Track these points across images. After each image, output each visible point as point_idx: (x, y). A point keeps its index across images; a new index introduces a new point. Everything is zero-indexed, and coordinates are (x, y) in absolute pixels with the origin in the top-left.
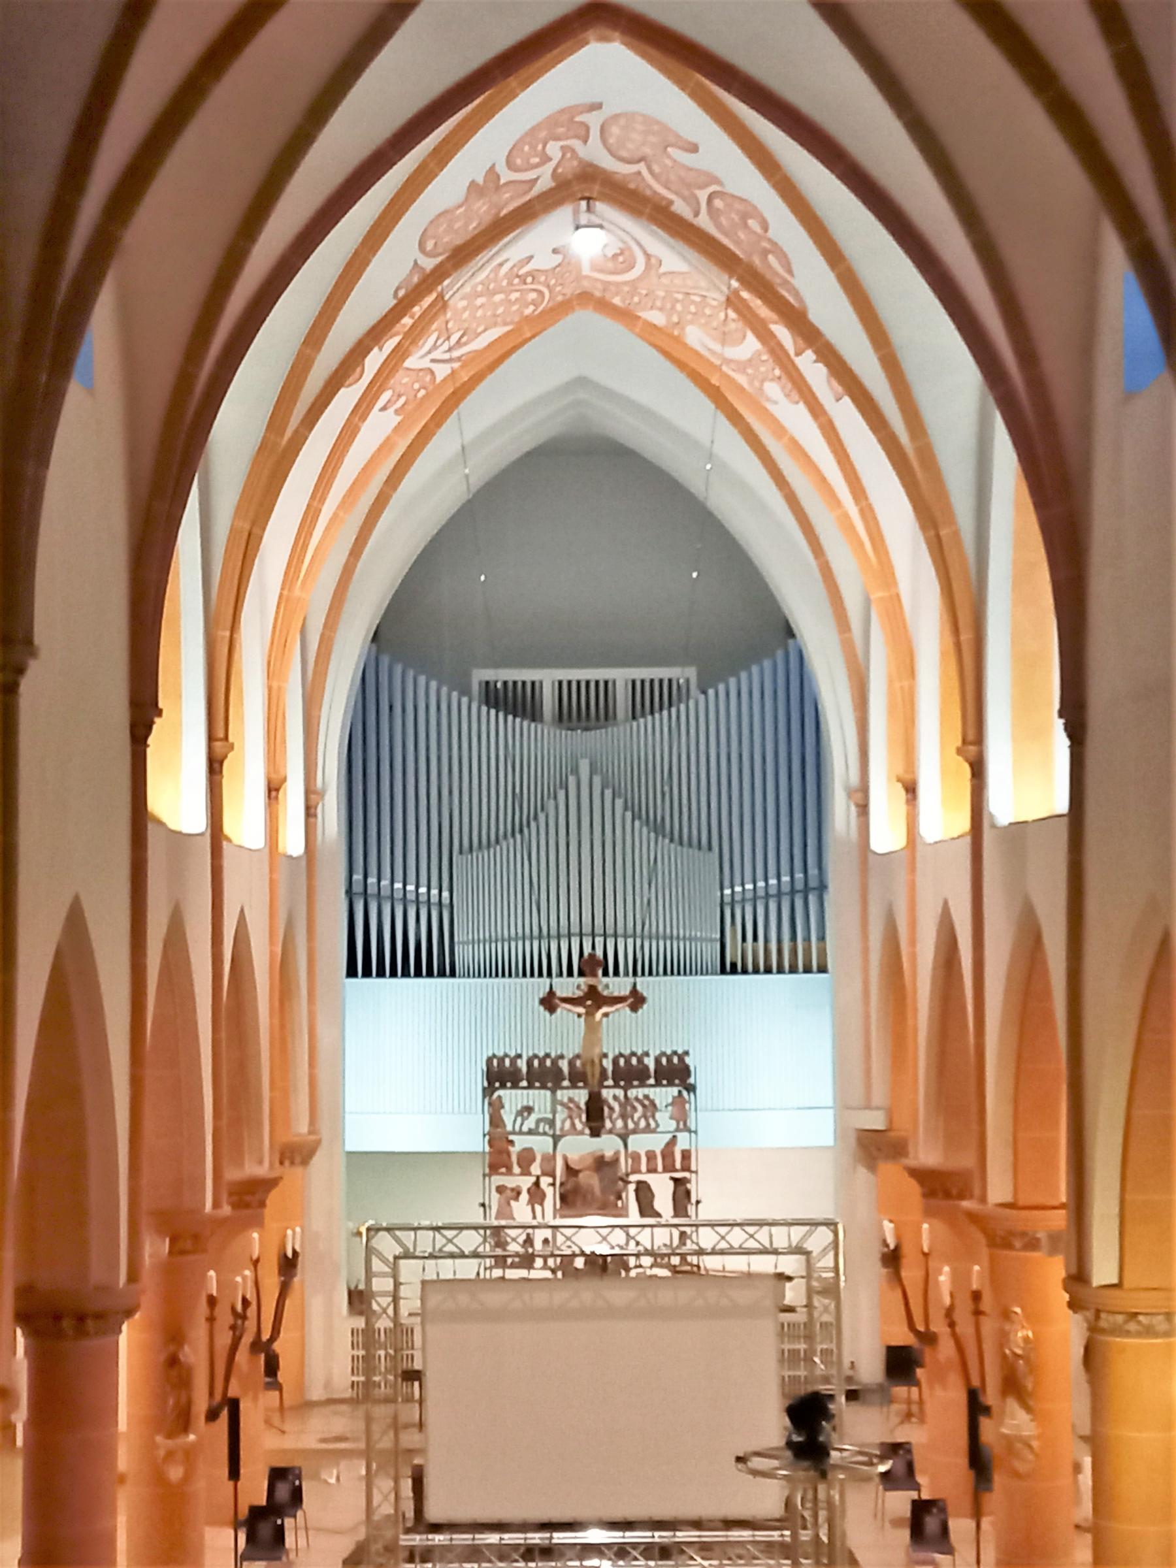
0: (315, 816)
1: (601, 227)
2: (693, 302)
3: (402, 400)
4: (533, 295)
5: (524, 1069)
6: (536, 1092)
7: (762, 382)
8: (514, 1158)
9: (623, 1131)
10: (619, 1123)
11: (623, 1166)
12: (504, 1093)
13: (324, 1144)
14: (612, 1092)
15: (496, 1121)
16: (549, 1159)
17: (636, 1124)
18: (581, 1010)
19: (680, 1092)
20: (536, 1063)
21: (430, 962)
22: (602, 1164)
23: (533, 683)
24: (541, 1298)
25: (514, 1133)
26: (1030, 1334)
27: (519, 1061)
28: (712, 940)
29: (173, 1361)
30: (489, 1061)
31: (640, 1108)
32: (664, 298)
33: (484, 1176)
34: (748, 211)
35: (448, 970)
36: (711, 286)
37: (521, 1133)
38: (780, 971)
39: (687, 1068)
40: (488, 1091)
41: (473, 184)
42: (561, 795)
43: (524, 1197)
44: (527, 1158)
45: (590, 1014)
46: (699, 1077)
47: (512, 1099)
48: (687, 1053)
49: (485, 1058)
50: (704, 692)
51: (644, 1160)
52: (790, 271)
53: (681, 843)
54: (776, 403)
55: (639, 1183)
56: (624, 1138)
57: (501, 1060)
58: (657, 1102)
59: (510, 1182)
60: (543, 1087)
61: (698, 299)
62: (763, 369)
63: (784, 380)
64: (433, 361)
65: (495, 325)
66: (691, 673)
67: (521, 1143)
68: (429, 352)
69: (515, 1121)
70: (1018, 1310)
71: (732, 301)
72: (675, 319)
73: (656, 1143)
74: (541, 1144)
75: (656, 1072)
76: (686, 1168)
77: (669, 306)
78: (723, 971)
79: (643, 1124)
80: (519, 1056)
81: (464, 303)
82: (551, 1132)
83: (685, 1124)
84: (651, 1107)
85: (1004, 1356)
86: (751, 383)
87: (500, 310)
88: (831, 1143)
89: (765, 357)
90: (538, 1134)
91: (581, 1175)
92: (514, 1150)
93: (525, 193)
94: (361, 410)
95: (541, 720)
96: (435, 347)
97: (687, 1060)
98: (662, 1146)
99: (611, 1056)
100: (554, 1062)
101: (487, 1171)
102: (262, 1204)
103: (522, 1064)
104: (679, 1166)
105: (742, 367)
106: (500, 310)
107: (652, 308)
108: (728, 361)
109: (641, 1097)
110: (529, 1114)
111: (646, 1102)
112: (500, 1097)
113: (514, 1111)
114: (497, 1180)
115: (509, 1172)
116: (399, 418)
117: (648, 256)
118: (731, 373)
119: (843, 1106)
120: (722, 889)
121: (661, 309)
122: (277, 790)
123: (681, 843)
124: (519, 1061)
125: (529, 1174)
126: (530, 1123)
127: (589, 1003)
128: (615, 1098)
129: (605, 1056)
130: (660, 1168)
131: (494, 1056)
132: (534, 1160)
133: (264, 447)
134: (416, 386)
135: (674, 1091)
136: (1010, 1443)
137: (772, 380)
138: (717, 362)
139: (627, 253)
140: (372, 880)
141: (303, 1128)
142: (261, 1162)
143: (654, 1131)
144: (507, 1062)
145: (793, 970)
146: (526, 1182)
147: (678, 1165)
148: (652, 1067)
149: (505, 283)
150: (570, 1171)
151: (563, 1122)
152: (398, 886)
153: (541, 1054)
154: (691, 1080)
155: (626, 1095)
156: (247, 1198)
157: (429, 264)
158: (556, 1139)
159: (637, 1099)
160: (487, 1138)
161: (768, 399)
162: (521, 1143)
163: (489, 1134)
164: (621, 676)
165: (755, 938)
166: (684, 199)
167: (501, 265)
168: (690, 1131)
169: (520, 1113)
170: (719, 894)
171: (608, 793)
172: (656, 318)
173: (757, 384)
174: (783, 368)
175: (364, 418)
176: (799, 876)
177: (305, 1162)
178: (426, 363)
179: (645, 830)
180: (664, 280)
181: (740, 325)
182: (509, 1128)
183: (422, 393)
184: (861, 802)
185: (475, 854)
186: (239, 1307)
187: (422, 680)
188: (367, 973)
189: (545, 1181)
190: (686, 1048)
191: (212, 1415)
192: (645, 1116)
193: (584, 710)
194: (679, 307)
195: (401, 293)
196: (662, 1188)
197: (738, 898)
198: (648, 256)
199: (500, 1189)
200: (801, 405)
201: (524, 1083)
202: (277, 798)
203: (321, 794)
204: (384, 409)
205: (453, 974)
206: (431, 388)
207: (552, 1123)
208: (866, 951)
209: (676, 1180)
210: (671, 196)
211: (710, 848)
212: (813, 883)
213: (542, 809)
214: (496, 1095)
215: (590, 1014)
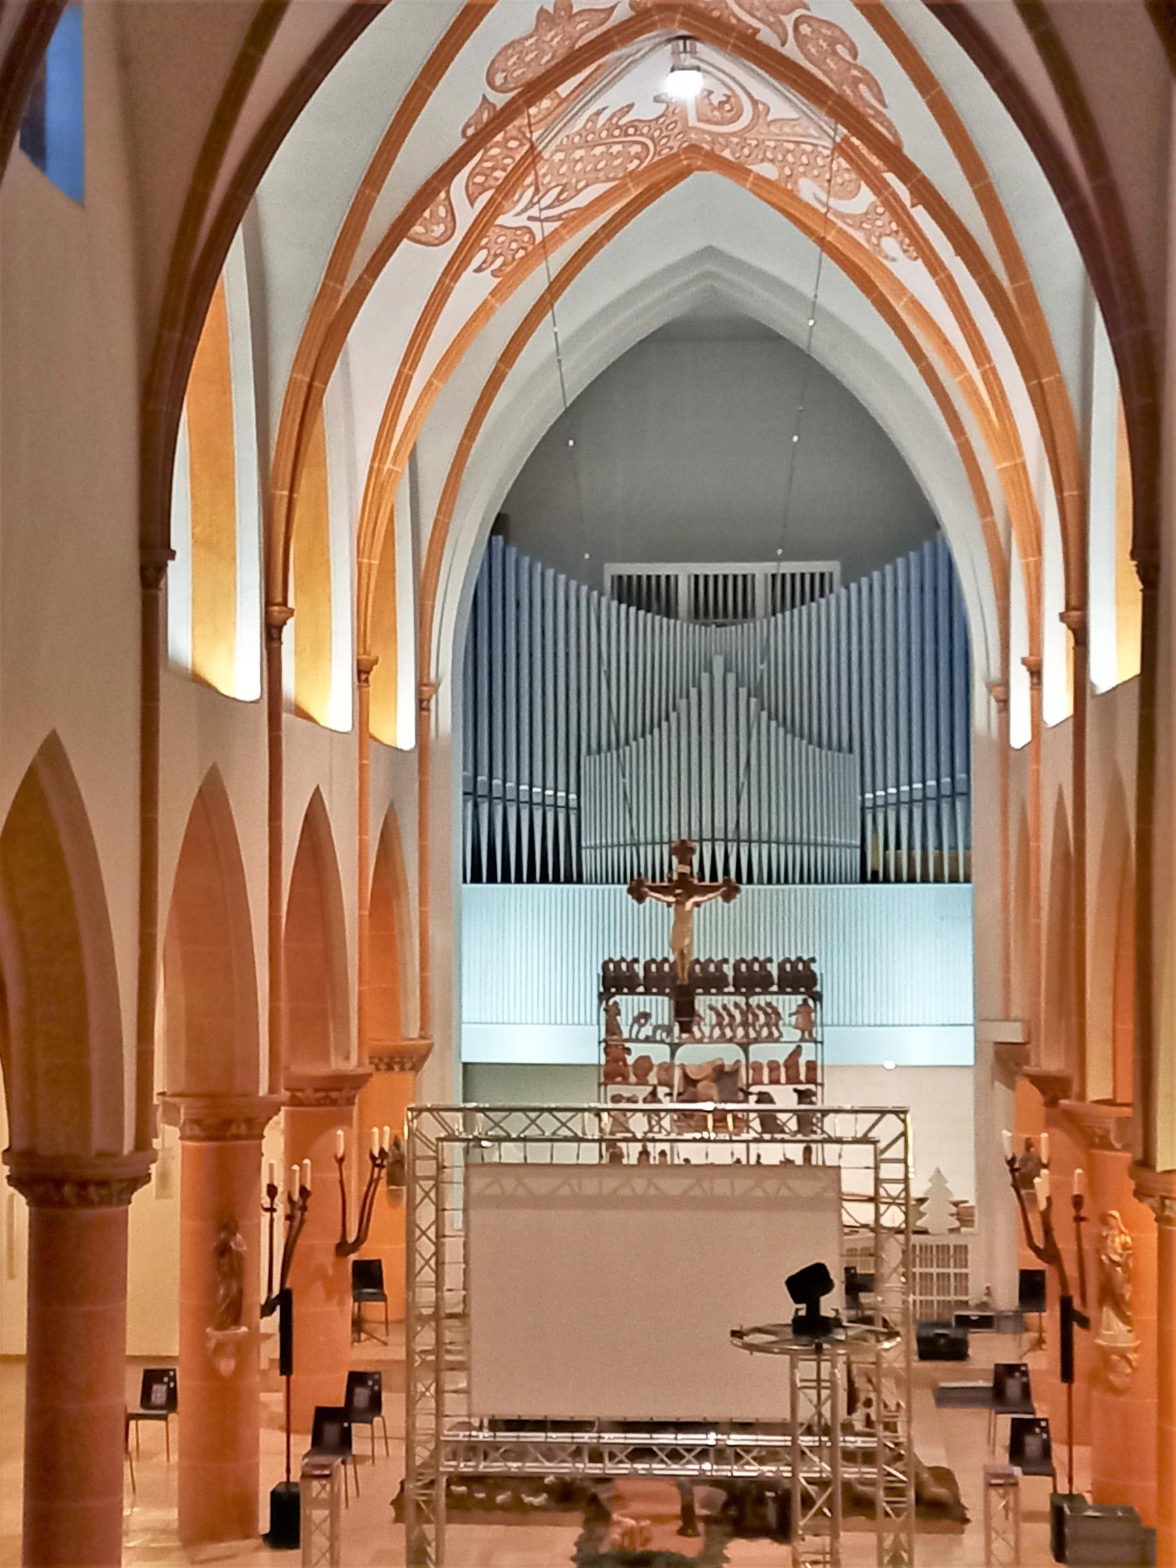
0: (428, 709)
1: (698, 69)
2: (804, 152)
3: (500, 260)
4: (636, 149)
5: (641, 974)
6: (654, 998)
7: (879, 238)
9: (745, 1040)
10: (740, 1032)
14: (733, 998)
15: (612, 1028)
17: (758, 1033)
18: (671, 899)
19: (805, 1001)
20: (653, 968)
21: (556, 867)
23: (668, 577)
24: (590, 1186)
25: (630, 1040)
26: (1129, 1240)
27: (636, 966)
28: (850, 846)
29: (224, 1250)
30: (605, 965)
31: (762, 1018)
32: (775, 148)
33: (600, 1085)
34: (837, 37)
36: (820, 133)
37: (637, 1040)
38: (925, 880)
39: (813, 975)
40: (604, 996)
41: (542, 11)
42: (693, 692)
44: (644, 1065)
45: (680, 903)
46: (825, 986)
47: (628, 1005)
48: (813, 960)
49: (601, 962)
50: (847, 588)
51: (766, 1071)
52: (882, 102)
53: (820, 745)
54: (894, 260)
55: (760, 1094)
56: (745, 1047)
57: (617, 964)
58: (780, 1010)
60: (661, 993)
61: (809, 148)
62: (879, 223)
63: (901, 234)
64: (530, 218)
65: (597, 180)
66: (832, 567)
67: (637, 1051)
68: (526, 209)
69: (632, 1026)
70: (1116, 1213)
71: (840, 149)
72: (787, 171)
73: (781, 1053)
74: (659, 1054)
75: (779, 978)
76: (811, 1080)
77: (780, 157)
78: (863, 880)
79: (765, 1032)
80: (636, 960)
81: (560, 156)
82: (668, 1040)
83: (810, 1034)
84: (773, 1015)
85: (1101, 1262)
86: (868, 241)
87: (601, 165)
88: (970, 1060)
89: (880, 210)
90: (656, 1042)
91: (700, 1085)
92: (630, 1060)
93: (601, 24)
94: (453, 271)
95: (676, 618)
96: (531, 204)
97: (814, 967)
98: (786, 1056)
99: (732, 961)
101: (602, 1079)
102: (350, 1102)
103: (639, 969)
104: (805, 1078)
105: (858, 222)
106: (601, 165)
107: (762, 161)
108: (843, 216)
109: (763, 1004)
111: (769, 1011)
112: (616, 1003)
113: (630, 1021)
114: (613, 1090)
115: (625, 1080)
116: (498, 280)
117: (755, 102)
118: (851, 231)
119: (981, 1018)
120: (863, 793)
121: (772, 161)
122: (368, 673)
123: (820, 745)
124: (636, 966)
125: (646, 1084)
126: (647, 1031)
127: (678, 891)
128: (736, 1005)
129: (726, 961)
130: (783, 1079)
131: (611, 960)
133: (325, 295)
134: (514, 246)
135: (800, 999)
136: (1105, 1355)
137: (889, 235)
138: (823, 210)
139: (732, 99)
140: (497, 782)
141: (414, 1032)
142: (347, 1058)
143: (777, 1041)
144: (624, 966)
145: (939, 879)
147: (802, 1077)
148: (775, 973)
149: (604, 134)
152: (524, 787)
153: (659, 959)
154: (818, 988)
155: (747, 1004)
156: (334, 1095)
157: (500, 100)
158: (674, 1048)
159: (759, 1007)
160: (603, 1045)
161: (886, 257)
162: (637, 1051)
163: (605, 1041)
164: (760, 570)
165: (898, 846)
166: (770, 25)
167: (598, 113)
168: (816, 1042)
169: (636, 1020)
170: (859, 798)
171: (743, 692)
172: (768, 171)
173: (874, 240)
174: (900, 222)
175: (456, 278)
176: (946, 780)
177: (416, 1068)
178: (522, 221)
179: (781, 730)
180: (774, 129)
181: (853, 175)
182: (626, 1035)
183: (521, 253)
184: (1002, 697)
185: (603, 755)
186: (296, 1196)
187: (550, 573)
188: (492, 879)
189: (662, 1091)
190: (811, 955)
191: (267, 1310)
192: (767, 1024)
193: (721, 604)
194: (790, 158)
195: (470, 132)
196: (784, 1097)
197: (880, 802)
198: (755, 102)
200: (920, 262)
201: (641, 989)
202: (367, 680)
203: (435, 687)
204: (479, 270)
205: (580, 881)
206: (530, 248)
208: (1006, 855)
210: (756, 24)
211: (851, 750)
212: (960, 788)
213: (674, 709)
214: (611, 1002)
215: (680, 903)
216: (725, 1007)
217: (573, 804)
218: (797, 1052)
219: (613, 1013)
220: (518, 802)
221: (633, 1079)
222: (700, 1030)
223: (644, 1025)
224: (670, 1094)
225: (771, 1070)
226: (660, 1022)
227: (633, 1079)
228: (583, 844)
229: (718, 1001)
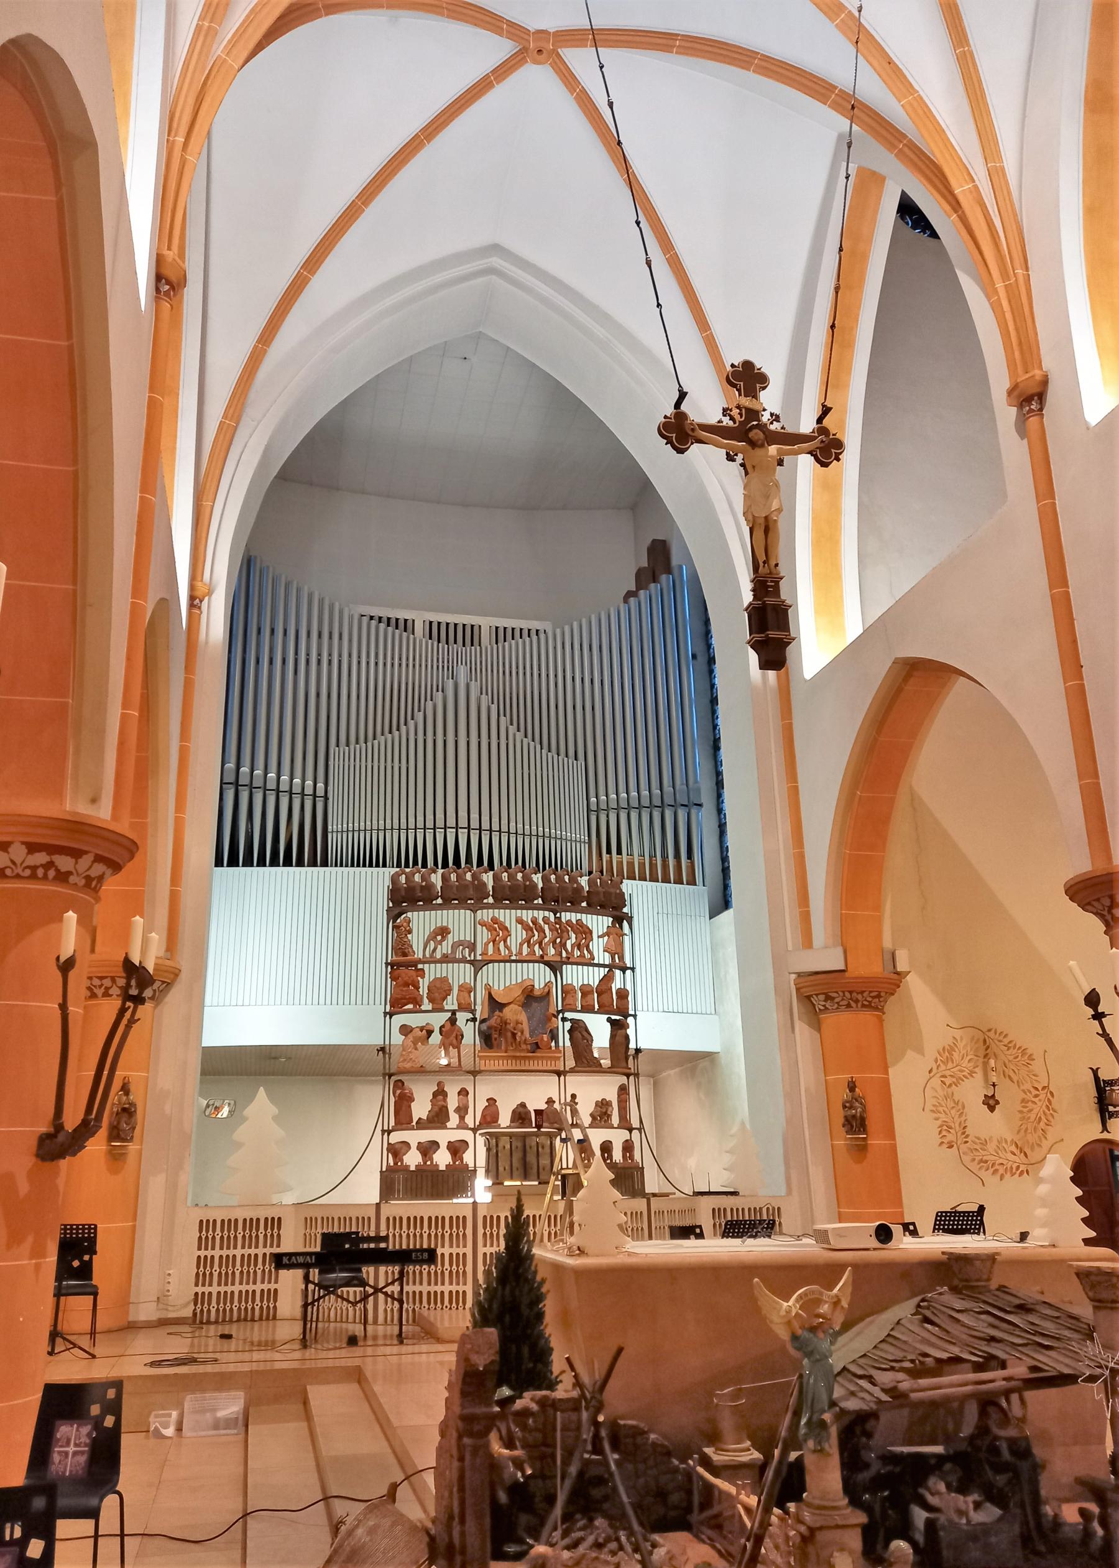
5: (439, 884)
8: (424, 990)
13: (184, 976)
15: (401, 947)
21: (303, 848)
22: (530, 997)
33: (385, 1013)
35: (320, 858)
37: (432, 961)
40: (394, 915)
43: (436, 1038)
44: (439, 992)
59: (415, 1020)
73: (592, 977)
91: (506, 1010)
92: (424, 985)
110: (444, 938)
114: (399, 1020)
126: (445, 948)
128: (546, 920)
132: (448, 992)
135: (607, 921)
140: (245, 769)
146: (438, 1020)
150: (495, 1005)
151: (487, 944)
152: (272, 775)
154: (625, 910)
159: (569, 922)
162: (432, 971)
168: (624, 969)
169: (433, 936)
189: (462, 1017)
196: (599, 1028)
199: (405, 1030)
205: (325, 864)
207: (472, 947)
216: (535, 921)
217: (320, 791)
218: (607, 979)
220: (265, 790)
221: (427, 1005)
222: (506, 946)
223: (440, 942)
224: (474, 1020)
225: (584, 995)
226: (462, 938)
227: (427, 1005)
228: (330, 827)
229: (527, 915)
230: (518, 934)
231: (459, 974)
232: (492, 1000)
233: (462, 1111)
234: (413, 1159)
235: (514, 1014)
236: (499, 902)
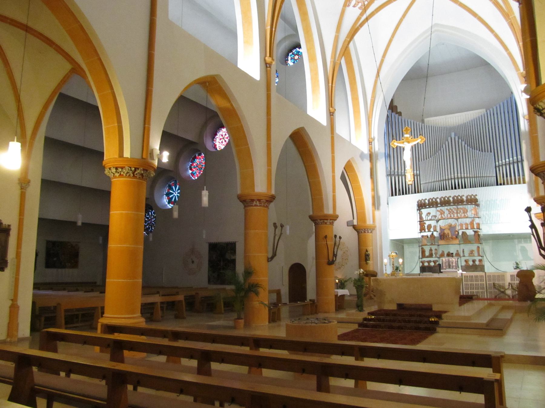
8: (426, 228)
11: (458, 228)
12: (422, 210)
15: (421, 218)
16: (435, 227)
22: (451, 227)
30: (418, 202)
37: (428, 220)
44: (429, 227)
48: (476, 195)
60: (433, 207)
67: (427, 223)
74: (433, 223)
78: (497, 185)
79: (463, 215)
84: (465, 211)
92: (426, 226)
97: (477, 197)
100: (436, 199)
103: (427, 201)
115: (425, 232)
126: (430, 217)
130: (469, 228)
132: (431, 227)
141: (371, 223)
143: (467, 217)
147: (475, 227)
162: (427, 223)
165: (507, 176)
171: (460, 140)
192: (464, 213)
196: (470, 232)
203: (374, 139)
209: (475, 232)
211: (491, 152)
216: (451, 209)
218: (473, 221)
219: (421, 214)
221: (427, 230)
227: (427, 230)
229: (449, 207)
230: (447, 212)
231: (433, 223)
232: (440, 228)
233: (436, 254)
234: (426, 264)
235: (446, 232)
236: (442, 206)
